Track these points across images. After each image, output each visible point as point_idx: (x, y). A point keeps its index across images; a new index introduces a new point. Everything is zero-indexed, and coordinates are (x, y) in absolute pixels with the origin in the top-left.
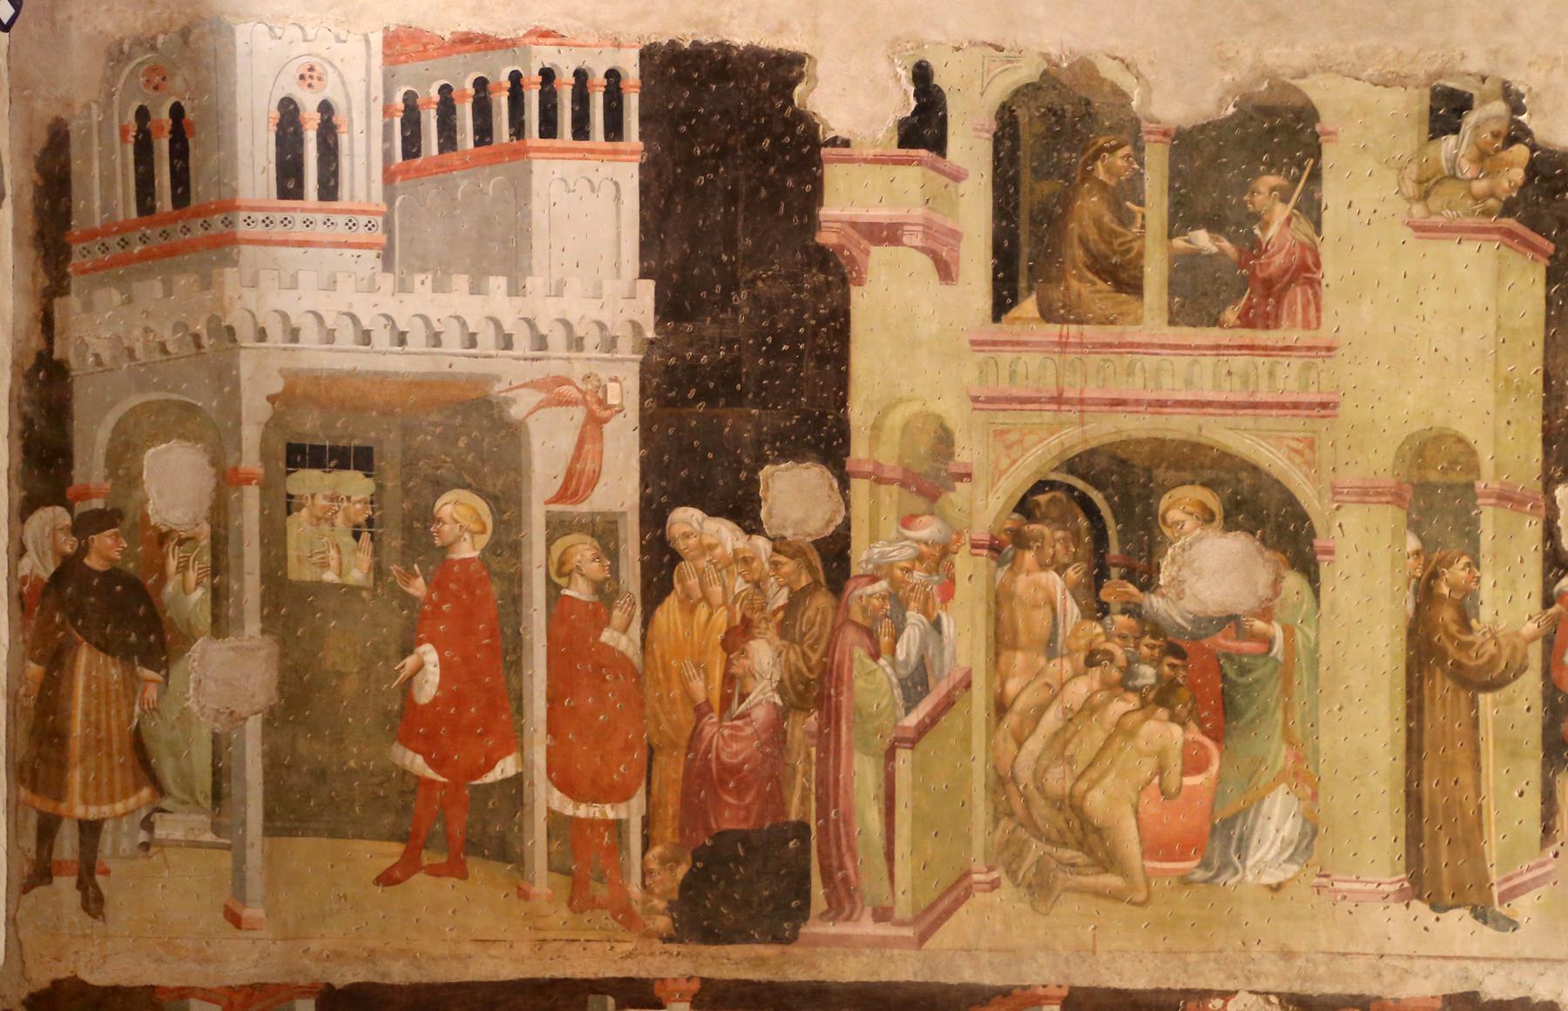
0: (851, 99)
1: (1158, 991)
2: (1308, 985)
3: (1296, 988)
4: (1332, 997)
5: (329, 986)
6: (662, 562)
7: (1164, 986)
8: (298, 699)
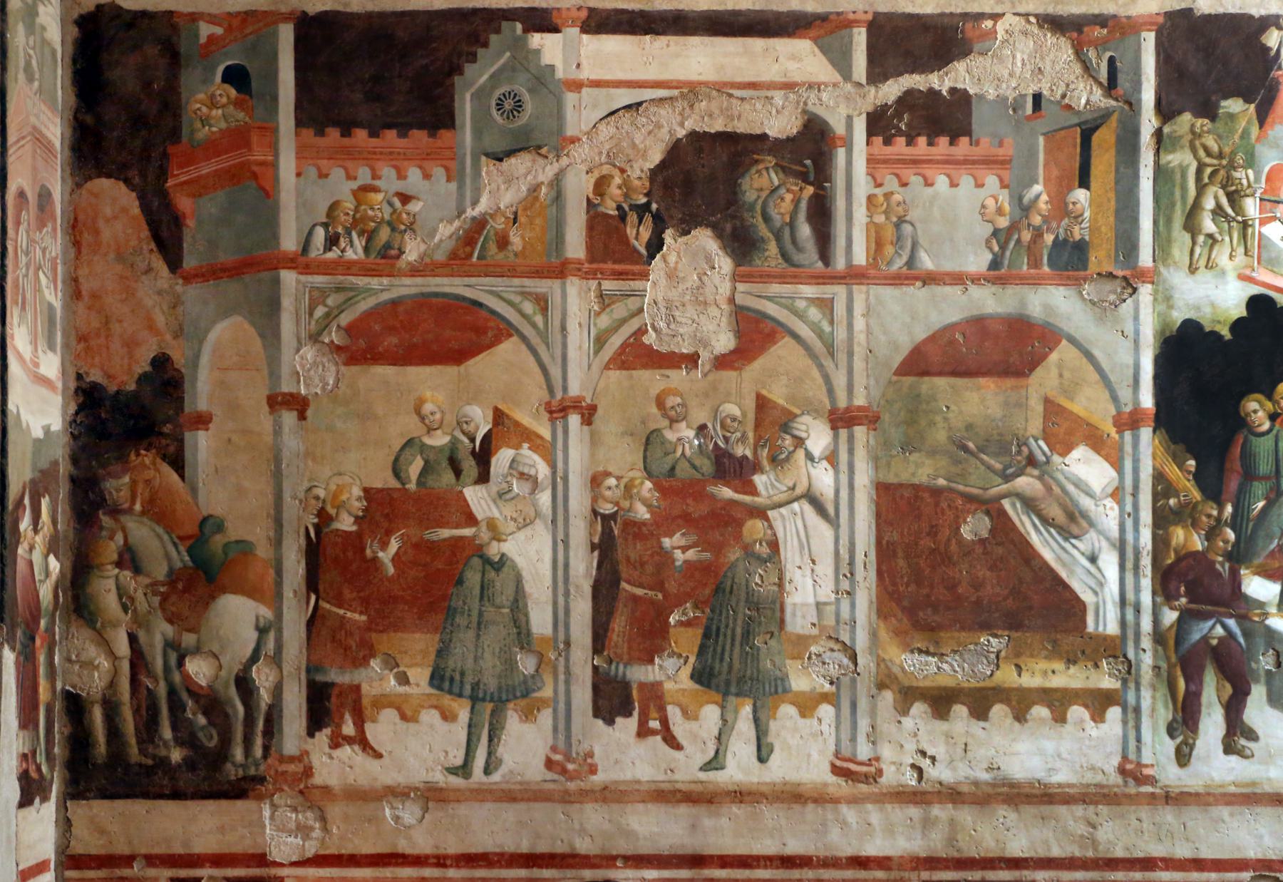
1: (942, 15)
2: (1059, 7)
3: (1050, 10)
4: (1079, 16)
5: (304, 13)
7: (947, 11)
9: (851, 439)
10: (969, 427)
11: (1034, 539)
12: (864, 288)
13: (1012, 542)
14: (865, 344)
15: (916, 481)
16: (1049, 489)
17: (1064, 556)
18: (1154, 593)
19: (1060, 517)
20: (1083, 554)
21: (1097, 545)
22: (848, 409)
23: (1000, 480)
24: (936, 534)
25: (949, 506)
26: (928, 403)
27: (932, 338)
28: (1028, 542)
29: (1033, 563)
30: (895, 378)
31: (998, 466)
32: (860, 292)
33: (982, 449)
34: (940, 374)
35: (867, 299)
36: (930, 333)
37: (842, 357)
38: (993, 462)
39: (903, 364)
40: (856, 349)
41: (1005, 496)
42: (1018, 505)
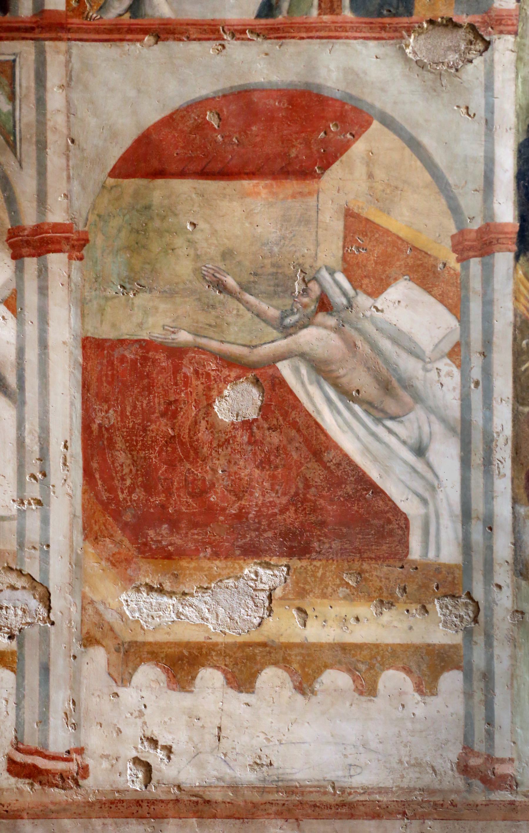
9: (43, 273)
10: (227, 254)
11: (329, 421)
12: (62, 45)
13: (294, 425)
14: (65, 131)
15: (144, 335)
16: (352, 346)
17: (374, 445)
18: (515, 501)
19: (369, 388)
20: (404, 443)
21: (426, 429)
22: (38, 229)
23: (275, 333)
24: (175, 415)
25: (196, 372)
26: (163, 218)
27: (169, 121)
28: (318, 425)
29: (326, 457)
30: (111, 181)
31: (273, 312)
32: (56, 53)
33: (245, 288)
34: (182, 175)
35: (68, 62)
36: (167, 112)
37: (28, 150)
38: (263, 306)
39: (124, 159)
40: (51, 137)
41: (283, 357)
42: (304, 370)
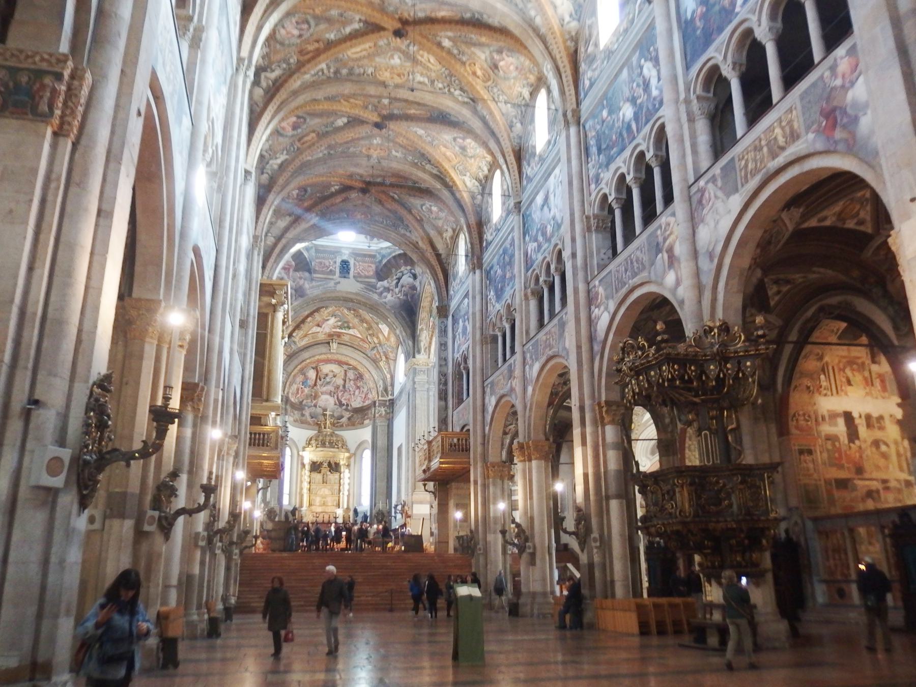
0: (855, 415)
6: (850, 448)
8: (829, 457)
